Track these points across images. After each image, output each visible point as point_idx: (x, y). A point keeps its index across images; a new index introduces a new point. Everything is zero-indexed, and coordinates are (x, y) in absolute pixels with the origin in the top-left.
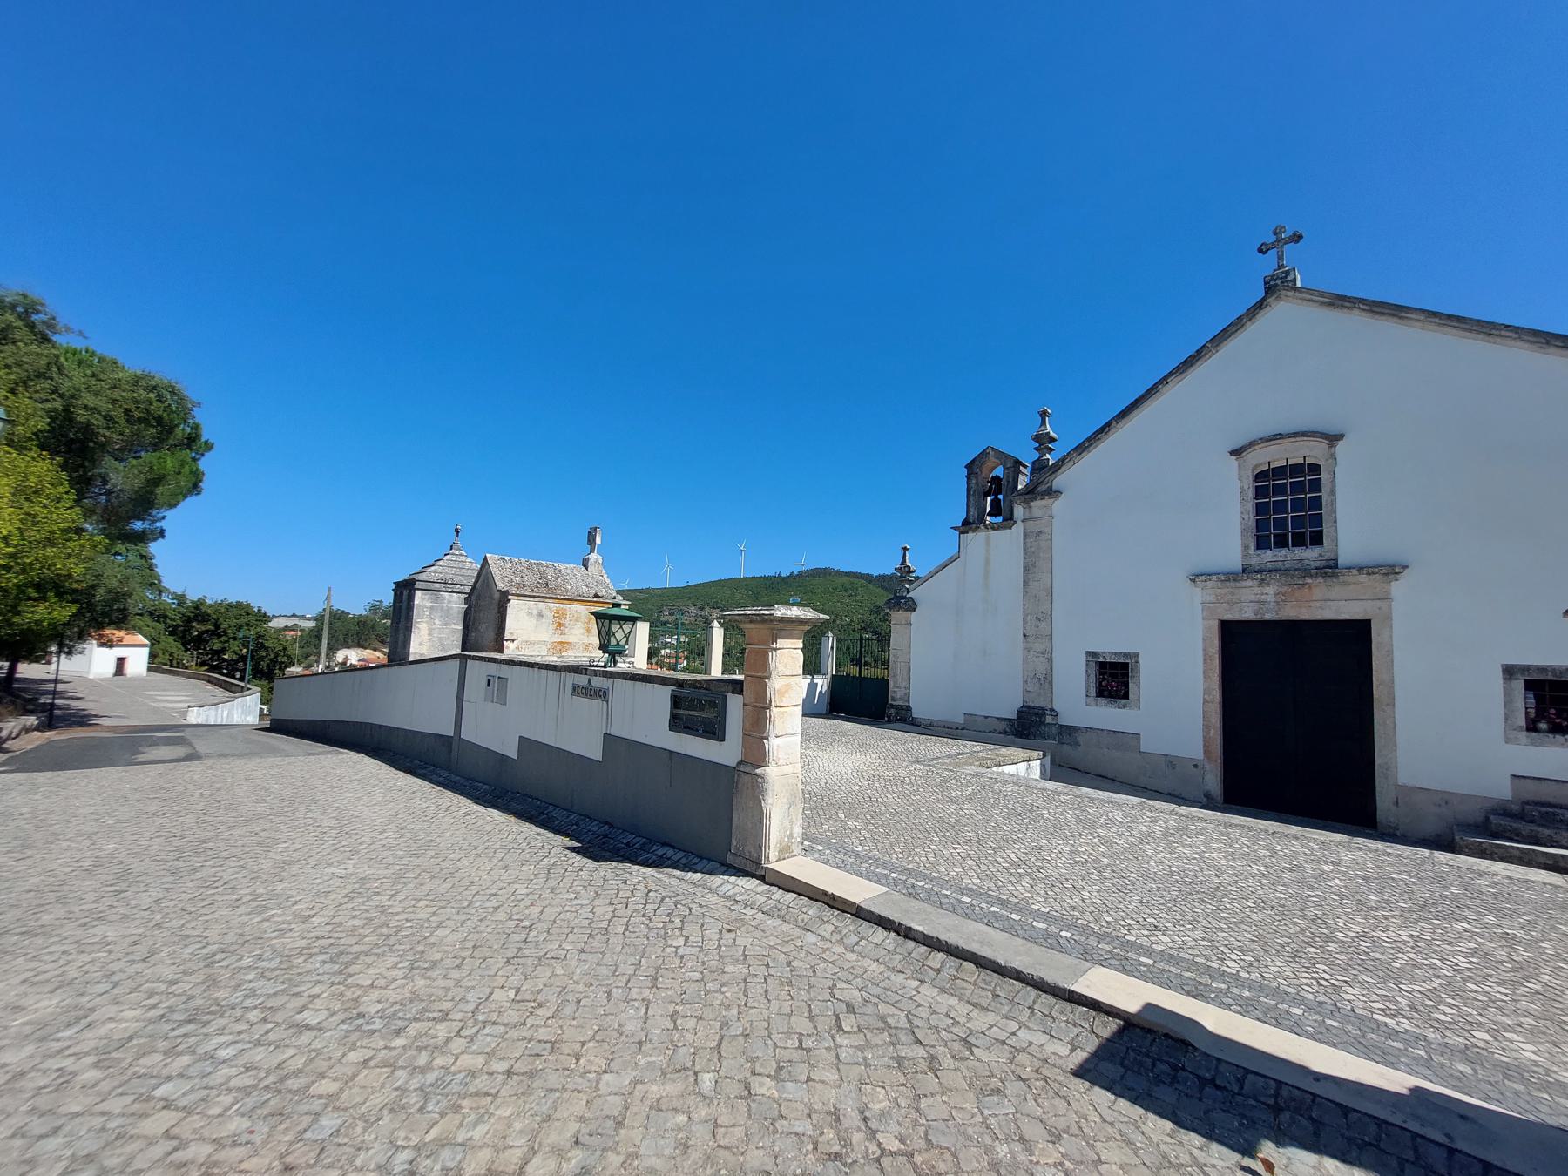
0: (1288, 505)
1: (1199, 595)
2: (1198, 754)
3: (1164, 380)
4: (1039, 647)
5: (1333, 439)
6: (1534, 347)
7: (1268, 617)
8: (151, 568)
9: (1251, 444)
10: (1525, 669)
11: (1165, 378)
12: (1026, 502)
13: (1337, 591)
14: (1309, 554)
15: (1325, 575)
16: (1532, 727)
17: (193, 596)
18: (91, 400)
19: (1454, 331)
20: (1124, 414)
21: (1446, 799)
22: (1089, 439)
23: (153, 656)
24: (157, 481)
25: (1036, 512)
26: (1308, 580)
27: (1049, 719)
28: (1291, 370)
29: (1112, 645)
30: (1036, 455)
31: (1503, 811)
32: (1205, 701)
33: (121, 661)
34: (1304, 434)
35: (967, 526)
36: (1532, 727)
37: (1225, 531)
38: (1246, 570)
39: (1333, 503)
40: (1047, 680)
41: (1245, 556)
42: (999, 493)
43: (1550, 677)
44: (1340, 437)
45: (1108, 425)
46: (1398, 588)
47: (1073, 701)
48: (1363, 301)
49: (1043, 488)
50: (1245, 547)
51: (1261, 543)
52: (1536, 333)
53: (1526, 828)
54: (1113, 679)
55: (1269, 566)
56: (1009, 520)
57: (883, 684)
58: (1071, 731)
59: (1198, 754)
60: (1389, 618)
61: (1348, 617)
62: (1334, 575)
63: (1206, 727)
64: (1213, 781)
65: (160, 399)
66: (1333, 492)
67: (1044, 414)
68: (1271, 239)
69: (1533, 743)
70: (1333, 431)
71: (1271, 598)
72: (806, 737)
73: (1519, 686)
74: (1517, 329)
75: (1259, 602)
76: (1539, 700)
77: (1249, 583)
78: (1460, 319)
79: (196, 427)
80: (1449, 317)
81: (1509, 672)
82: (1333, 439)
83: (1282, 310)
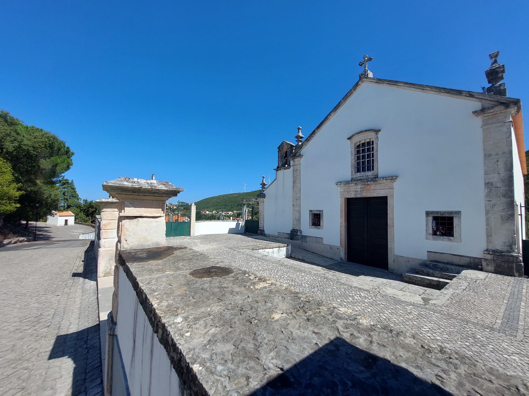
0: (364, 157)
1: (339, 189)
2: (338, 244)
3: (329, 114)
4: (297, 209)
5: (377, 131)
6: (436, 93)
7: (358, 196)
8: (75, 192)
9: (353, 136)
10: (432, 212)
11: (330, 113)
12: (293, 159)
13: (378, 187)
14: (370, 174)
15: (373, 181)
16: (435, 234)
17: (89, 200)
18: (26, 142)
19: (413, 89)
20: (318, 127)
21: (408, 260)
22: (309, 137)
23: (76, 219)
24: (56, 165)
25: (296, 163)
26: (369, 183)
27: (299, 233)
29: (316, 208)
30: (297, 143)
31: (425, 265)
32: (341, 226)
33: (66, 221)
34: (368, 130)
35: (278, 169)
36: (435, 234)
37: (346, 167)
38: (352, 180)
39: (377, 155)
40: (299, 220)
41: (352, 175)
42: (287, 156)
43: (439, 215)
44: (380, 131)
45: (314, 131)
46: (396, 184)
47: (306, 228)
48: (386, 80)
49: (298, 154)
50: (352, 172)
51: (358, 171)
52: (436, 88)
53: (426, 270)
54: (316, 219)
55: (359, 178)
56: (289, 165)
57: (258, 222)
58: (305, 237)
59: (338, 244)
60: (393, 195)
61: (381, 196)
62: (376, 181)
63: (341, 235)
64: (342, 254)
65: (50, 140)
66: (377, 151)
67: (299, 129)
68: (362, 60)
69: (434, 239)
70: (376, 128)
71: (359, 190)
72: (166, 240)
73: (430, 219)
74: (430, 87)
75: (357, 191)
76: (437, 224)
77: (352, 185)
78: (413, 84)
79: (68, 148)
80: (410, 84)
81: (428, 213)
82: (377, 131)
83: (364, 86)
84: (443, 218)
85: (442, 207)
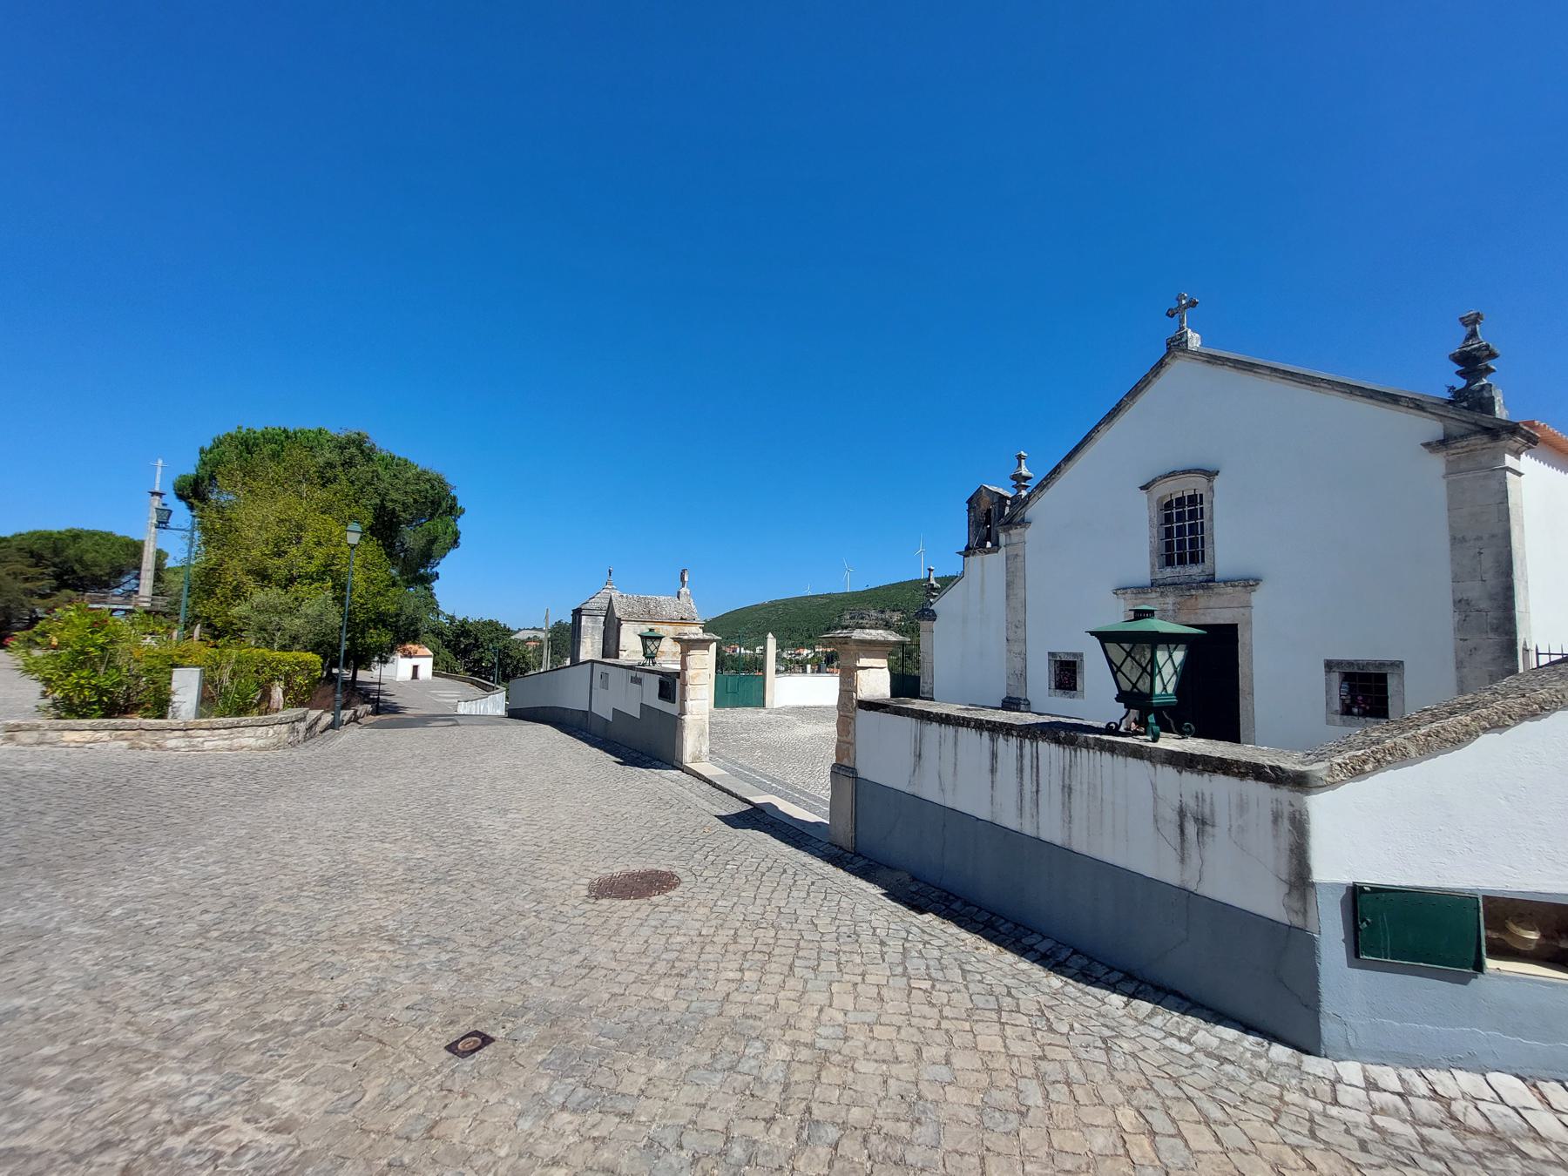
0: (1182, 531)
3: (1096, 429)
4: (1016, 649)
5: (1210, 474)
8: (432, 596)
9: (1154, 481)
10: (1339, 663)
13: (1213, 602)
14: (1194, 570)
15: (1203, 588)
16: (1347, 711)
17: (460, 617)
18: (394, 495)
20: (1069, 457)
23: (435, 664)
24: (432, 541)
25: (1015, 539)
28: (1190, 416)
33: (415, 668)
34: (1189, 472)
35: (968, 551)
36: (1347, 711)
37: (1137, 554)
38: (1154, 584)
39: (1212, 528)
40: (1022, 676)
42: (992, 521)
45: (1058, 466)
46: (1257, 597)
49: (1018, 519)
50: (1153, 566)
56: (996, 545)
60: (1249, 623)
65: (432, 487)
66: (1211, 519)
67: (1020, 457)
71: (1170, 607)
73: (1336, 677)
76: (1352, 690)
79: (454, 499)
81: (1330, 666)
82: (1210, 474)
83: (1178, 368)
84: (1366, 677)
85: (1362, 651)
